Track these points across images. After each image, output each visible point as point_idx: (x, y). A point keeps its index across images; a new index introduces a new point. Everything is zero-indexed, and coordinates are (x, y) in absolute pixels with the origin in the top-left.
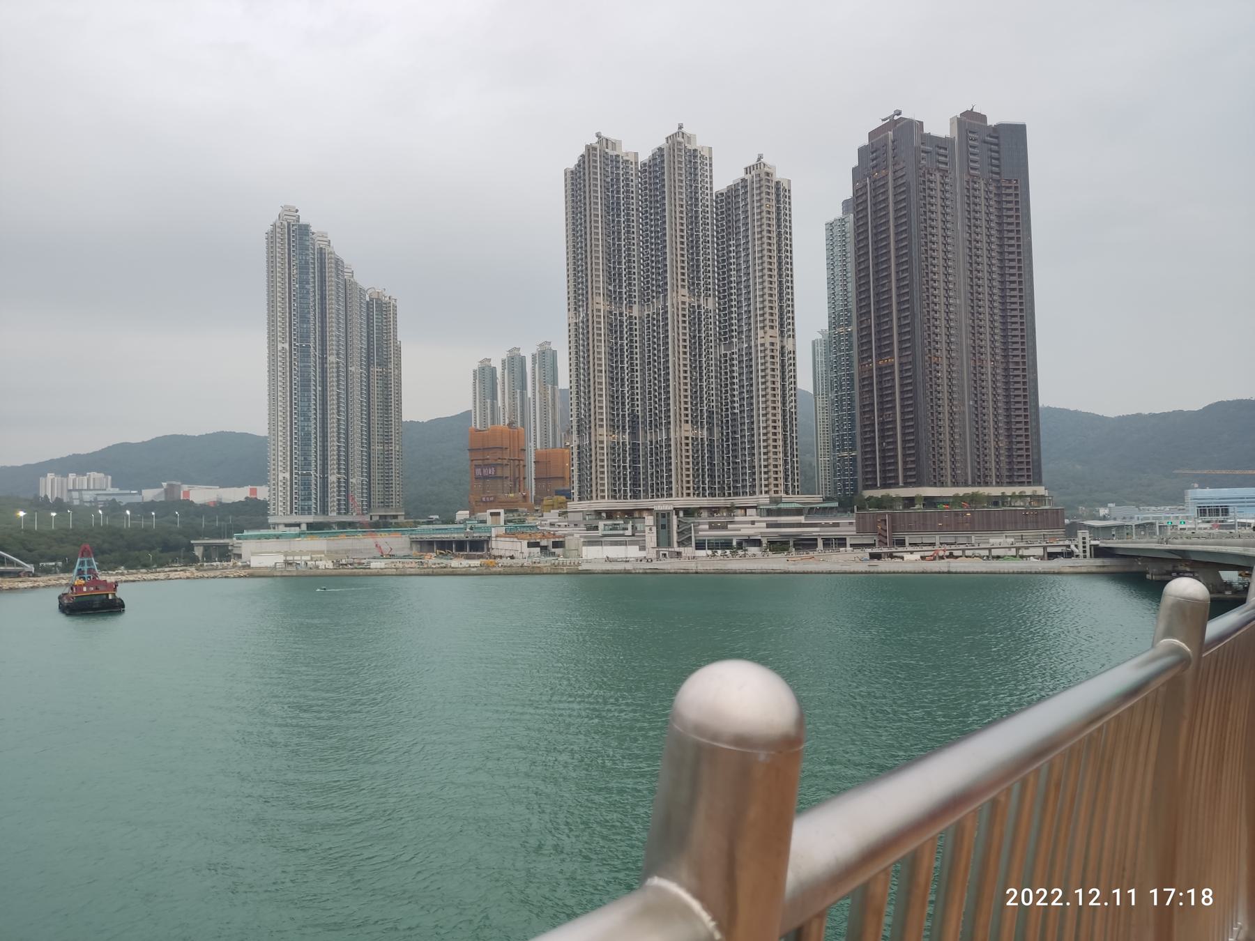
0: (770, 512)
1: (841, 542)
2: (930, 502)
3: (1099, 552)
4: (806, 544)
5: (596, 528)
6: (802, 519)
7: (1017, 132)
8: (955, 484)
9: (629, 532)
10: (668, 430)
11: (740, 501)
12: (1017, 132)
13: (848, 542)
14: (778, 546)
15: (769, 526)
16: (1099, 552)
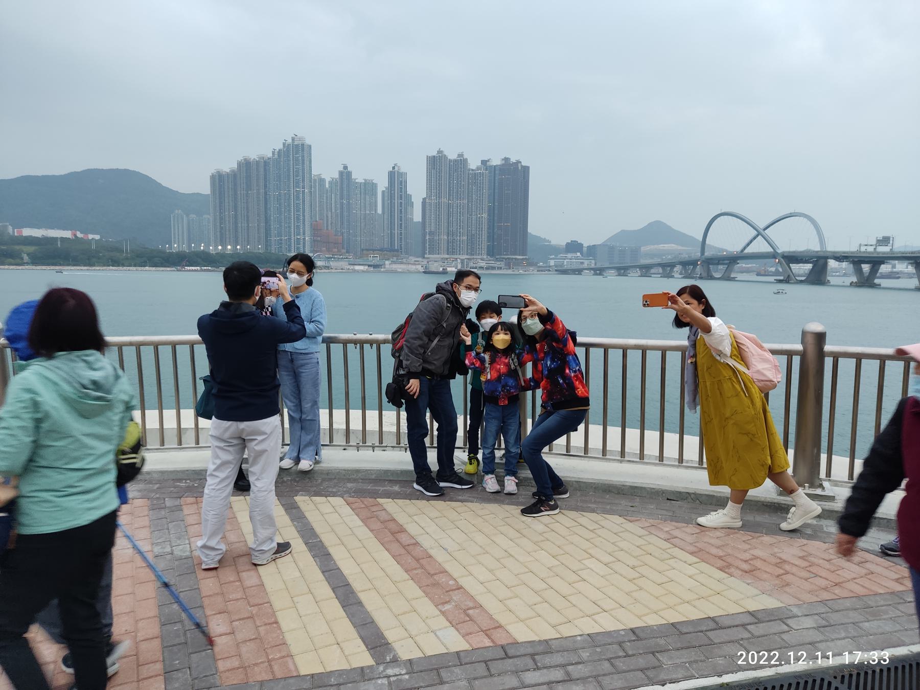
0: (486, 261)
1: (501, 268)
2: (515, 259)
3: (556, 270)
4: (493, 268)
5: (445, 263)
6: (493, 262)
7: (528, 168)
8: (519, 255)
9: (454, 264)
10: (460, 237)
11: (475, 257)
12: (528, 168)
13: (503, 268)
14: (487, 268)
15: (486, 263)
16: (556, 270)
